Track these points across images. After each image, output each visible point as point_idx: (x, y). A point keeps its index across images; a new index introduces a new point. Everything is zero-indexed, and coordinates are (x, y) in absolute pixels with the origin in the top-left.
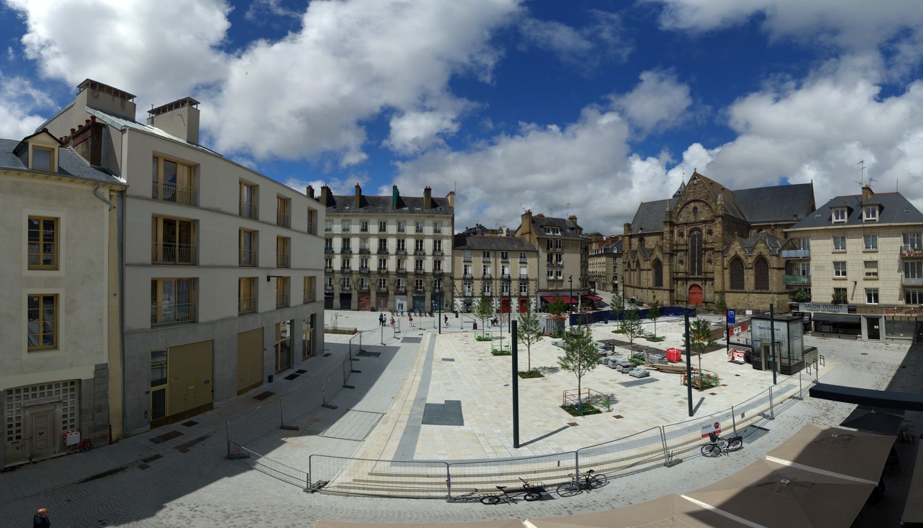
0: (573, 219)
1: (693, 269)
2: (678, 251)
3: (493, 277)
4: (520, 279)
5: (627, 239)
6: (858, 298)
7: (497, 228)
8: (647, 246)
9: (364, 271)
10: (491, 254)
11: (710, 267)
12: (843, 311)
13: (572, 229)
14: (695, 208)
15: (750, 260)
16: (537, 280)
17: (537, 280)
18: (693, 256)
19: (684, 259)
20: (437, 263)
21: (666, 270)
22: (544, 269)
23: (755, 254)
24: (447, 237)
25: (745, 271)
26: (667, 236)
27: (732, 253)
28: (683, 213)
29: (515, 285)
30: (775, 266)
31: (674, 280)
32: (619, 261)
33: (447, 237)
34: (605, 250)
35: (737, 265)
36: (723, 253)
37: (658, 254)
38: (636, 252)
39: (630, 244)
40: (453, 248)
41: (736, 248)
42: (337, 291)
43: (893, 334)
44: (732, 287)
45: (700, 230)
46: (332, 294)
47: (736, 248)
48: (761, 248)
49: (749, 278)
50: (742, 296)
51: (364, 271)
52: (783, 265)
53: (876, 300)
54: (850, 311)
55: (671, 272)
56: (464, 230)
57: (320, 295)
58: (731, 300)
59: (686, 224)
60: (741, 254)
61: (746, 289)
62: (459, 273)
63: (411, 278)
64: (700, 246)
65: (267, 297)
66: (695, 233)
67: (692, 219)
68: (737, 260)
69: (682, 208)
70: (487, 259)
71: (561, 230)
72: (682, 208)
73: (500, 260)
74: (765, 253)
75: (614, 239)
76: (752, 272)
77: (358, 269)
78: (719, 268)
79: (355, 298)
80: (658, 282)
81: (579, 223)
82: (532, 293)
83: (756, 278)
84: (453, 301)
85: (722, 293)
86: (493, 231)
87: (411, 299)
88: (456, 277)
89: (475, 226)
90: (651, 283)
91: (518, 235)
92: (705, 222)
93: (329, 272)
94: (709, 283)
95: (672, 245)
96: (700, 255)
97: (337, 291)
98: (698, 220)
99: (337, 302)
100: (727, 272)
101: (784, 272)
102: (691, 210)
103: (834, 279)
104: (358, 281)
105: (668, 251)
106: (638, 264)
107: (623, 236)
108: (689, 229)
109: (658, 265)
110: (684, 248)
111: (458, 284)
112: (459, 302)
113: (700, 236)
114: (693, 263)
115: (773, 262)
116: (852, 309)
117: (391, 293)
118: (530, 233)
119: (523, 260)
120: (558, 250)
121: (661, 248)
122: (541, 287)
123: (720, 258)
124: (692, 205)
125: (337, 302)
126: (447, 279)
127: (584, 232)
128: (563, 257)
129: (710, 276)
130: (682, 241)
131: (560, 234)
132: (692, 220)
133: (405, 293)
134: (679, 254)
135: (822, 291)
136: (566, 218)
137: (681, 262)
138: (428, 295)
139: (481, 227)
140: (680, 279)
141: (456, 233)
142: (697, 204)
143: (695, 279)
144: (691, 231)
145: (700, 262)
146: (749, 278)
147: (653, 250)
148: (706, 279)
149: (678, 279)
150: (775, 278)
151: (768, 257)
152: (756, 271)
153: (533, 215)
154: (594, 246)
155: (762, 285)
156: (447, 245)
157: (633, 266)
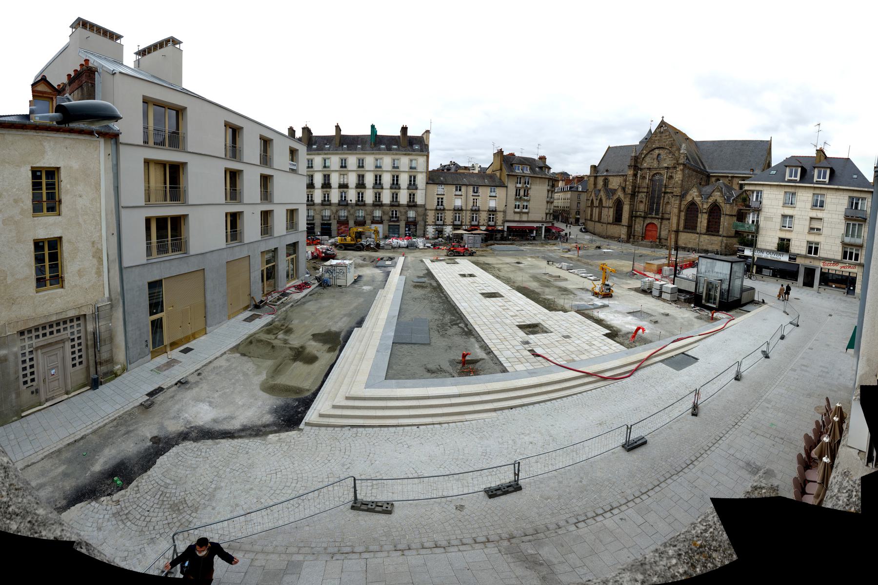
0: (543, 159)
1: (651, 209)
2: (639, 192)
3: (464, 208)
5: (592, 179)
6: (798, 246)
7: (470, 165)
8: (610, 186)
9: (343, 203)
10: (463, 189)
11: (669, 208)
12: (785, 258)
13: (541, 168)
14: (659, 154)
15: (705, 206)
16: (504, 212)
17: (504, 212)
18: (653, 198)
19: (644, 200)
20: (412, 196)
21: (626, 209)
22: (512, 202)
23: (711, 200)
24: (422, 172)
25: (700, 215)
26: (630, 179)
27: (689, 198)
28: (648, 159)
29: (483, 216)
30: (728, 213)
31: (632, 217)
32: (584, 197)
33: (422, 172)
34: (571, 188)
35: (692, 210)
36: (682, 196)
37: (620, 194)
38: (600, 191)
39: (595, 184)
40: (427, 183)
42: (318, 222)
43: (827, 284)
44: (685, 227)
46: (314, 224)
47: (693, 195)
48: (717, 196)
49: (703, 221)
50: (694, 236)
51: (343, 203)
52: (734, 213)
53: (816, 252)
54: (790, 258)
55: (631, 211)
56: (439, 166)
57: (303, 225)
58: (685, 238)
60: (698, 200)
61: (698, 231)
63: (388, 208)
64: (660, 190)
65: (251, 227)
66: (657, 177)
68: (693, 204)
69: (647, 154)
70: (458, 193)
71: (531, 169)
72: (647, 154)
74: (720, 200)
75: (580, 179)
76: (705, 216)
77: (337, 201)
78: (676, 211)
79: (334, 227)
80: (618, 219)
81: (548, 162)
83: (709, 222)
84: (425, 231)
85: (677, 232)
86: (466, 168)
87: (387, 227)
88: (428, 207)
89: (448, 163)
90: (611, 220)
91: (488, 172)
92: (667, 168)
93: (310, 203)
94: (665, 222)
95: (634, 186)
96: (659, 198)
97: (318, 222)
98: (661, 166)
99: (318, 231)
100: (683, 214)
101: (735, 219)
103: (781, 230)
104: (337, 211)
105: (630, 192)
106: (601, 200)
107: (589, 177)
110: (645, 190)
112: (431, 230)
113: (661, 181)
114: (652, 204)
115: (726, 209)
116: (793, 257)
117: (368, 222)
118: (501, 169)
119: (493, 194)
121: (624, 189)
122: (508, 218)
123: (678, 202)
125: (318, 231)
126: (420, 210)
127: (552, 171)
128: (531, 192)
129: (666, 216)
130: (644, 185)
131: (528, 172)
134: (640, 195)
135: (768, 239)
136: (536, 158)
138: (402, 224)
139: (455, 164)
140: (640, 216)
141: (430, 169)
143: (652, 218)
144: (653, 175)
145: (658, 204)
146: (703, 221)
147: (616, 190)
148: (662, 219)
149: (636, 217)
150: (726, 223)
151: (722, 205)
152: (709, 216)
153: (505, 154)
154: (561, 184)
155: (713, 228)
156: (421, 180)
157: (596, 203)
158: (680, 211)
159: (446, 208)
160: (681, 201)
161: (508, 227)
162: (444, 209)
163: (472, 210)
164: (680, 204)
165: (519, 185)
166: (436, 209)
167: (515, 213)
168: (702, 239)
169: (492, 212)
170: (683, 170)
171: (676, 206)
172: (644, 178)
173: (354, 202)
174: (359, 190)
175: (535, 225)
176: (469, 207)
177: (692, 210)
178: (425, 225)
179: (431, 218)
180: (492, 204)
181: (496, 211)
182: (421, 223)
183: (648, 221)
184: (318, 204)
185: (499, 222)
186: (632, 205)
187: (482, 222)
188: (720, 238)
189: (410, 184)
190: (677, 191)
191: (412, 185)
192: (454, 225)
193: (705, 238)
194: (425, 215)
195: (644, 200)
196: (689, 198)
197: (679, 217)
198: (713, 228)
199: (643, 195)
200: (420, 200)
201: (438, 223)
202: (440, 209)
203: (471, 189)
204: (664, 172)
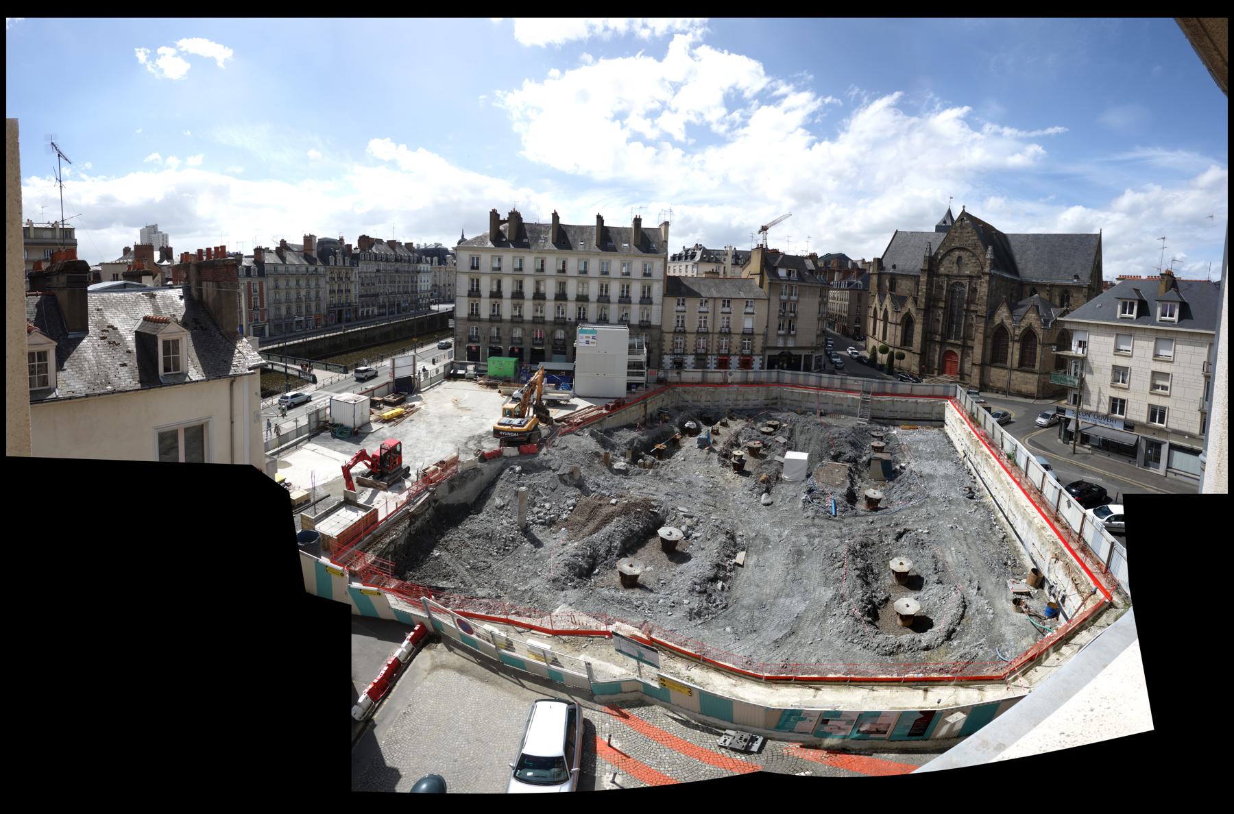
3: (710, 330)
4: (744, 334)
14: (960, 258)
15: (1018, 332)
16: (765, 335)
23: (1024, 324)
25: (1010, 344)
27: (997, 321)
29: (736, 340)
40: (664, 295)
41: (1003, 314)
45: (962, 285)
48: (1032, 318)
59: (947, 276)
60: (1008, 322)
61: (1009, 365)
62: (670, 325)
68: (1002, 328)
76: (1017, 346)
82: (758, 350)
88: (665, 328)
92: (970, 277)
100: (989, 341)
105: (922, 306)
109: (907, 322)
111: (668, 338)
113: (961, 293)
119: (749, 310)
120: (794, 298)
122: (770, 344)
126: (655, 333)
129: (969, 343)
132: (955, 272)
145: (959, 325)
155: (1026, 363)
156: (657, 290)
158: (986, 337)
159: (688, 330)
160: (986, 324)
161: (769, 357)
162: (685, 332)
163: (720, 333)
164: (986, 328)
165: (784, 297)
167: (779, 335)
168: (1013, 377)
169: (748, 335)
170: (989, 282)
171: (981, 330)
172: (941, 287)
173: (573, 320)
174: (580, 304)
175: (803, 353)
176: (717, 330)
177: (998, 338)
178: (661, 355)
179: (667, 346)
180: (748, 324)
181: (752, 334)
184: (528, 322)
185: (758, 350)
186: (926, 324)
187: (734, 350)
188: (1036, 376)
189: (643, 297)
190: (982, 309)
191: (646, 300)
192: (697, 354)
193: (1017, 376)
194: (661, 340)
196: (997, 321)
197: (984, 345)
198: (1026, 363)
200: (655, 321)
201: (677, 351)
202: (681, 332)
204: (965, 282)
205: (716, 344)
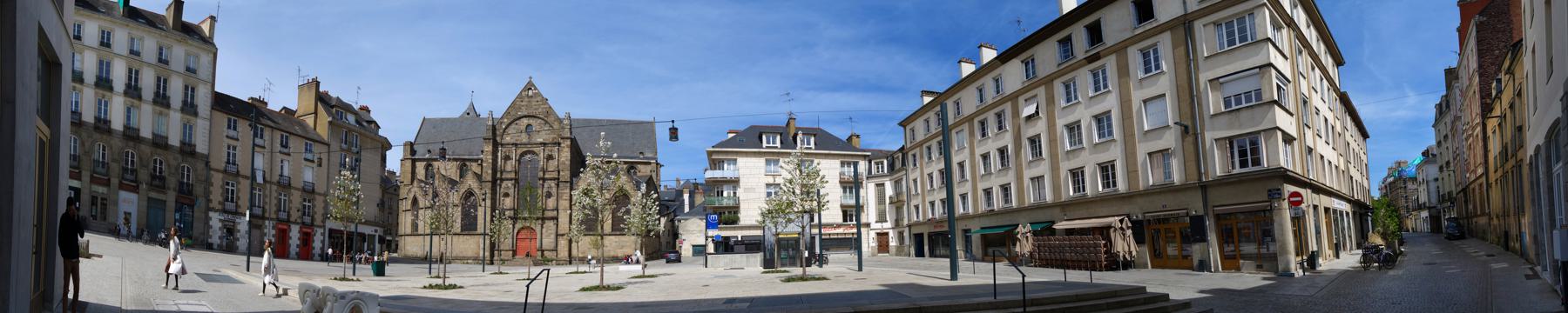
2: (502, 180)
19: (511, 191)
28: (511, 130)
62: (219, 161)
67: (524, 138)
73: (278, 147)
84: (208, 219)
88: (213, 164)
102: (523, 128)
108: (520, 151)
110: (513, 175)
117: (115, 181)
124: (525, 121)
132: (525, 140)
133: (135, 189)
137: (507, 195)
142: (531, 121)
144: (522, 155)
166: (225, 171)
172: (507, 158)
176: (276, 178)
182: (201, 202)
183: (518, 226)
194: (208, 182)
195: (511, 191)
199: (510, 184)
202: (231, 173)
203: (278, 135)
205: (274, 202)
